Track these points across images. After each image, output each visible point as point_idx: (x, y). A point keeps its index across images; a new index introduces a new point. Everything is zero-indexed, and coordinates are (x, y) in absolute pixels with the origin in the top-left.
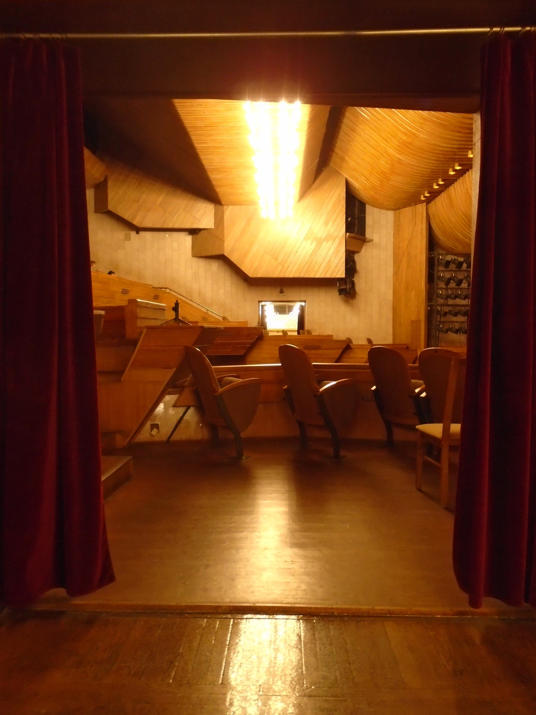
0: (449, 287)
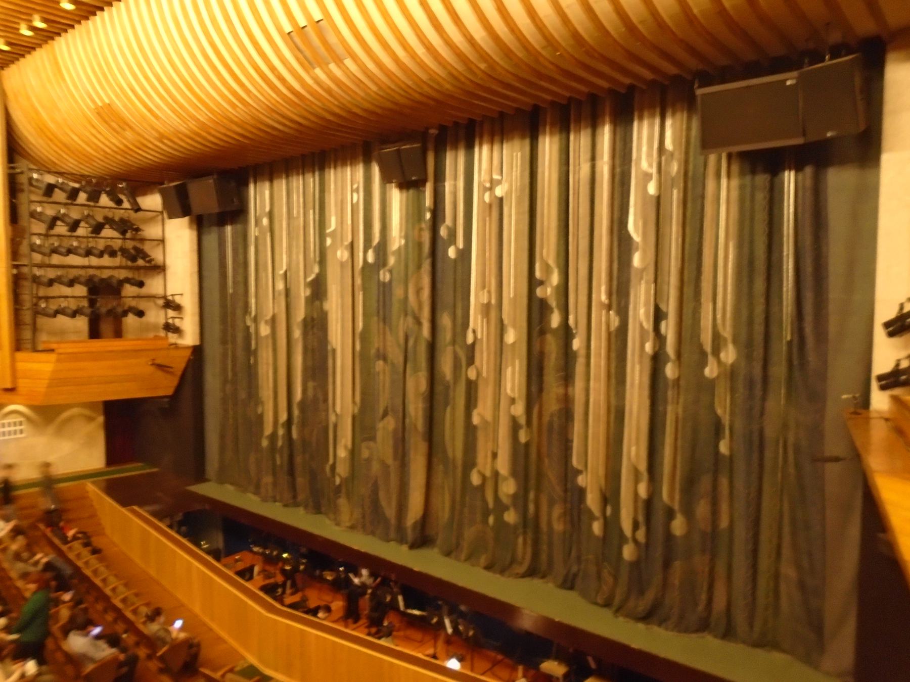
0: (53, 232)
